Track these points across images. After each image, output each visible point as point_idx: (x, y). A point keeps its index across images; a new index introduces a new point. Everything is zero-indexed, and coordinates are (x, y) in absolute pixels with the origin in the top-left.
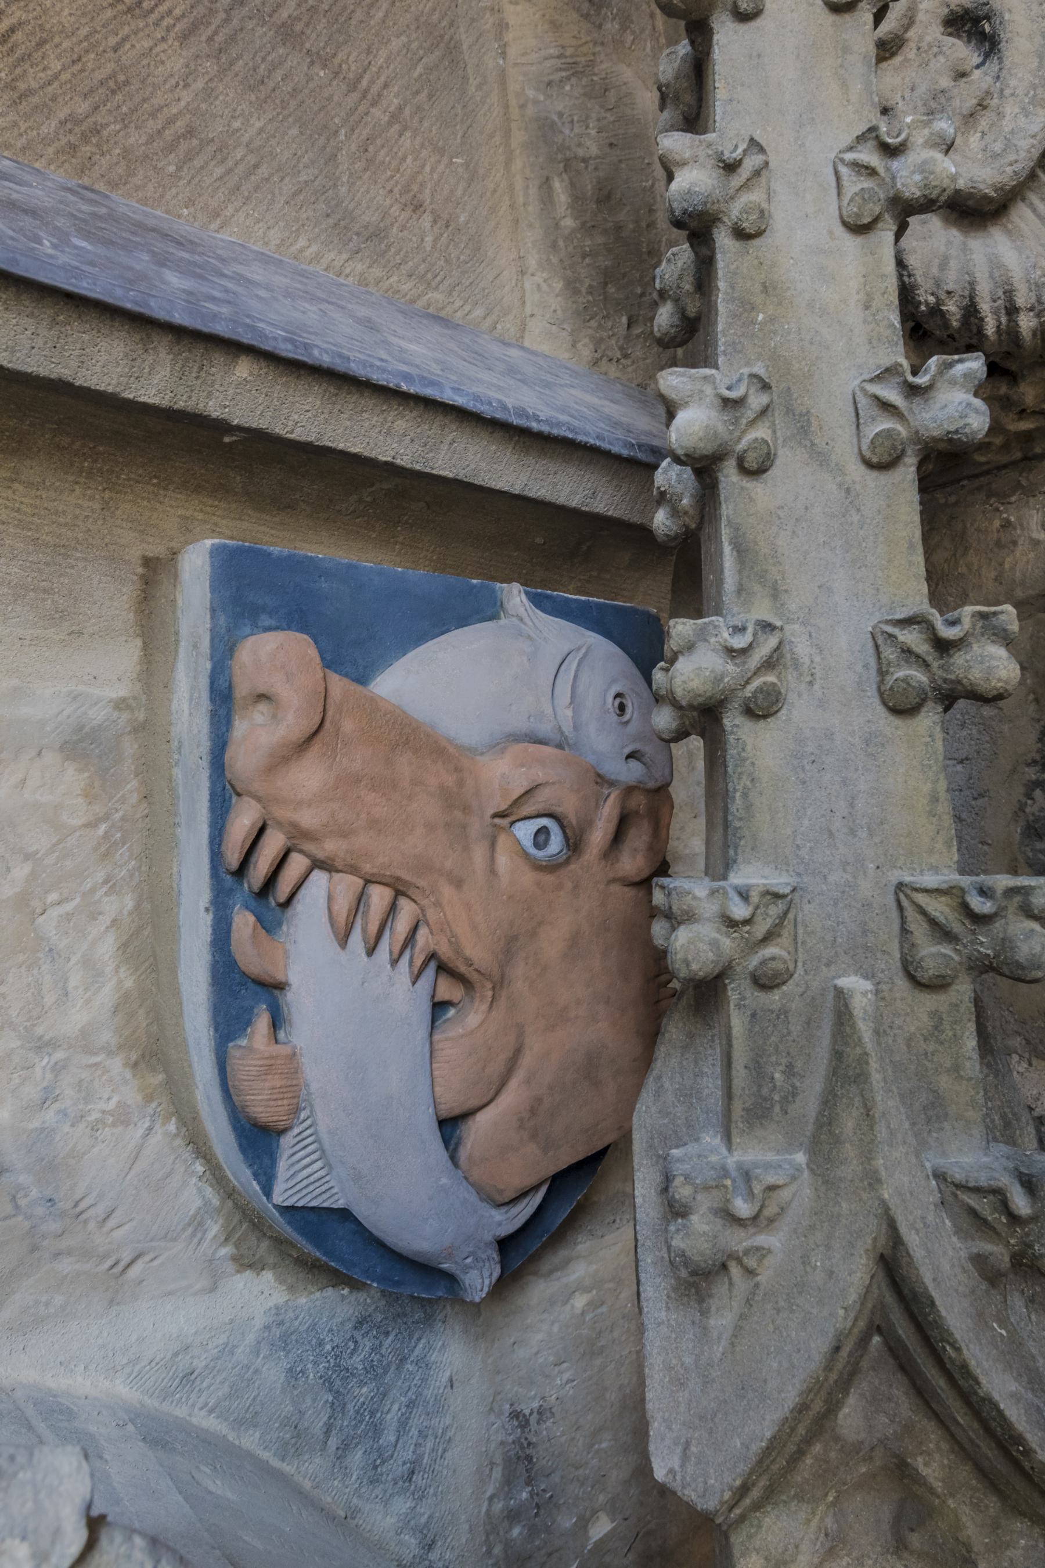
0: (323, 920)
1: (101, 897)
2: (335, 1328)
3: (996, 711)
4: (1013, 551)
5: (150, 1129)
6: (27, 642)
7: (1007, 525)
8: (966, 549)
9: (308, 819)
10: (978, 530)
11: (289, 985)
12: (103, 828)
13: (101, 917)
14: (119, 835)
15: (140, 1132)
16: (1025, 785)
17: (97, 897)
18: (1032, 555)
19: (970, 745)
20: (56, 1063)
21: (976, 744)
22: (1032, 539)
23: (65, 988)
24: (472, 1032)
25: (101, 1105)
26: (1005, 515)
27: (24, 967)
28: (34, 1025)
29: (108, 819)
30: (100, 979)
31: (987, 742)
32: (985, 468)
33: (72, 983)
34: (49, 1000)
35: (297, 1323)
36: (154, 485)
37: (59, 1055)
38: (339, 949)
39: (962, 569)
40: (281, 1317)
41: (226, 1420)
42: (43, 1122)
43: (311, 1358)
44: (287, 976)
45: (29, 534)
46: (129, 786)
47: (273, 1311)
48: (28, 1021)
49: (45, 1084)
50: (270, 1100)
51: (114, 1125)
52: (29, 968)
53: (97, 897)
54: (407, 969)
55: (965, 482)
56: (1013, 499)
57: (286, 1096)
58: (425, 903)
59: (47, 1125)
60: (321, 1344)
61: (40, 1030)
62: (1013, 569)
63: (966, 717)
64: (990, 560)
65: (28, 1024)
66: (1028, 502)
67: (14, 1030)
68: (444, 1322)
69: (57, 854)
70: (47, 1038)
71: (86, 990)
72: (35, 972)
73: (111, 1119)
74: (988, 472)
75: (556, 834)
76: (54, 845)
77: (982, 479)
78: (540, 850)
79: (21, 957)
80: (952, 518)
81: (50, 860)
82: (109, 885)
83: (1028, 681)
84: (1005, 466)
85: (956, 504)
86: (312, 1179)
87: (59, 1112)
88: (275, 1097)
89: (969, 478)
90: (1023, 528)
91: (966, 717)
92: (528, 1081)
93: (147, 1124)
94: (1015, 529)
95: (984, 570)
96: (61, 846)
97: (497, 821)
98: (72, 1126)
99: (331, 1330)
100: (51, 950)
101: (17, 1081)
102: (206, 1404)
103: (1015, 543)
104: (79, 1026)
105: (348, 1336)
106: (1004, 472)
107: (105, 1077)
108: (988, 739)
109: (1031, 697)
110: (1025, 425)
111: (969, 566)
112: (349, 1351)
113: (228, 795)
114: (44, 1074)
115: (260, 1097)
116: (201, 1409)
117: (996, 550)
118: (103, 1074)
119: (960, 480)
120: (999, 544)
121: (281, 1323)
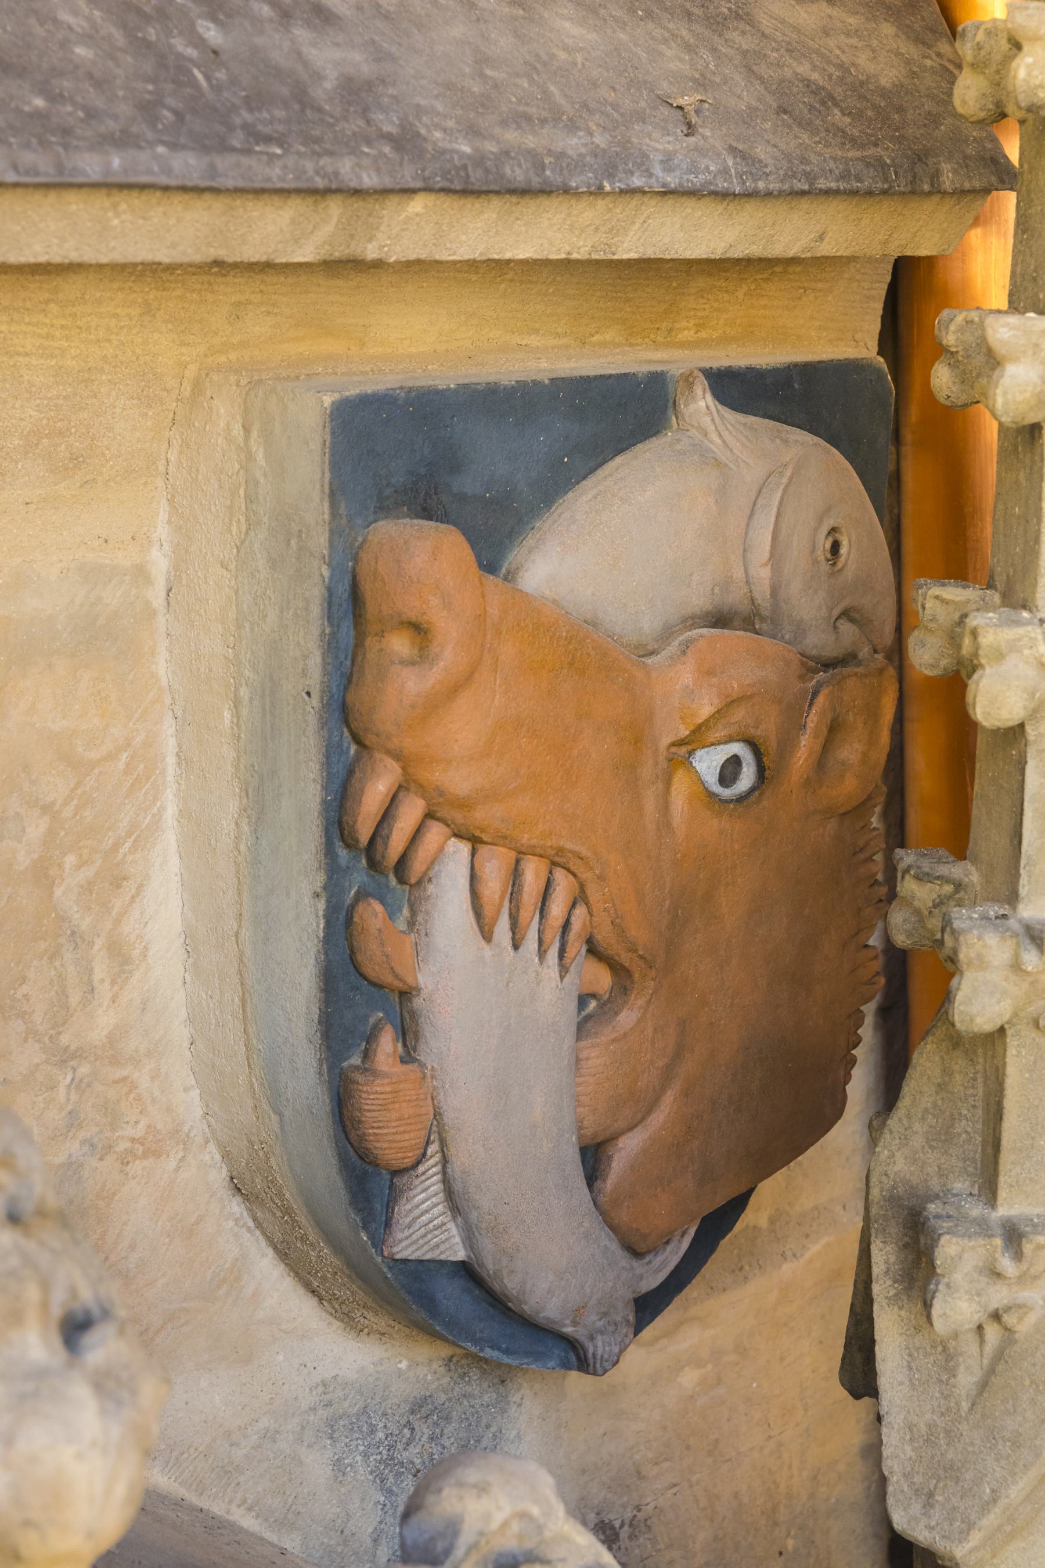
0: (465, 907)
1: (125, 855)
2: (390, 1411)
5: (183, 1159)
6: (33, 507)
9: (459, 781)
11: (419, 990)
12: (124, 757)
13: (125, 883)
14: (142, 766)
15: (173, 1164)
17: (120, 857)
20: (81, 1080)
23: (90, 982)
24: (625, 1035)
25: (129, 1131)
27: (45, 958)
28: (59, 1033)
29: (129, 745)
30: (126, 967)
33: (97, 977)
34: (74, 1000)
35: (346, 1404)
36: (215, 274)
37: (84, 1069)
38: (483, 942)
40: (328, 1397)
41: (266, 1520)
42: (70, 1156)
43: (361, 1448)
44: (416, 979)
45: (53, 363)
46: (151, 695)
47: (321, 1389)
48: (53, 1028)
49: (70, 1107)
50: (397, 1133)
51: (145, 1156)
52: (51, 958)
53: (120, 857)
54: (556, 960)
57: (413, 1127)
58: (586, 876)
59: (74, 1159)
60: (373, 1431)
61: (65, 1039)
65: (53, 1032)
67: (39, 1041)
68: (520, 1405)
69: (75, 802)
70: (72, 1048)
71: (113, 982)
72: (57, 963)
73: (141, 1149)
75: (748, 764)
76: (73, 790)
78: (727, 787)
79: (43, 945)
81: (67, 812)
82: (133, 838)
86: (431, 1226)
87: (83, 1143)
88: (402, 1129)
92: (686, 1093)
93: (181, 1154)
96: (79, 792)
97: (673, 749)
98: (101, 1159)
99: (385, 1414)
100: (73, 933)
101: (42, 1105)
102: (244, 1501)
104: (106, 1032)
105: (403, 1422)
107: (132, 1096)
112: (404, 1440)
113: (346, 745)
114: (68, 1094)
115: (385, 1131)
116: (239, 1506)
118: (131, 1091)
121: (329, 1404)
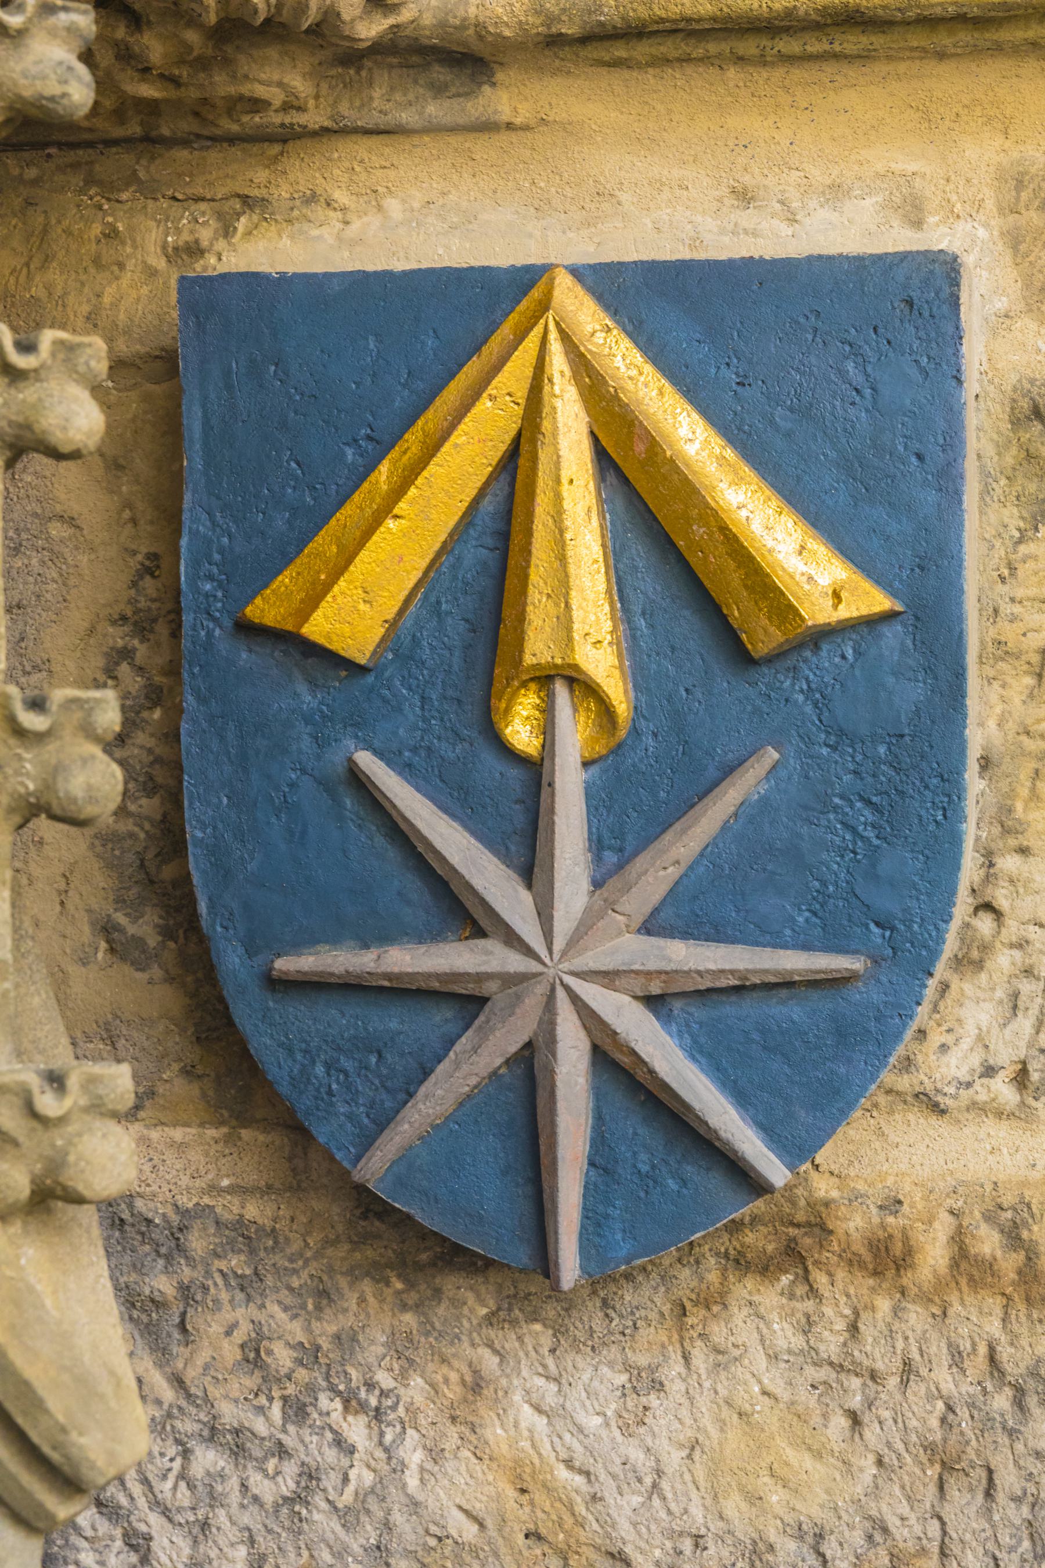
3: (72, 531)
4: (117, 278)
7: (111, 234)
8: (47, 259)
10: (68, 232)
16: (106, 654)
18: (145, 290)
19: (25, 583)
21: (36, 583)
22: (144, 262)
26: (110, 219)
31: (54, 581)
32: (87, 136)
39: (37, 290)
55: (52, 151)
56: (124, 196)
62: (115, 306)
63: (24, 536)
64: (83, 284)
66: (145, 207)
74: (90, 144)
77: (81, 152)
80: (29, 203)
83: (124, 488)
84: (111, 143)
85: (35, 182)
89: (60, 145)
90: (135, 247)
91: (24, 536)
94: (123, 243)
95: (71, 299)
103: (121, 266)
106: (114, 150)
108: (55, 575)
109: (127, 514)
110: (148, 91)
111: (49, 288)
117: (92, 270)
119: (46, 145)
120: (97, 261)
